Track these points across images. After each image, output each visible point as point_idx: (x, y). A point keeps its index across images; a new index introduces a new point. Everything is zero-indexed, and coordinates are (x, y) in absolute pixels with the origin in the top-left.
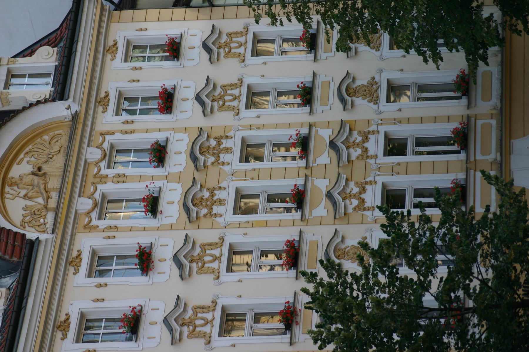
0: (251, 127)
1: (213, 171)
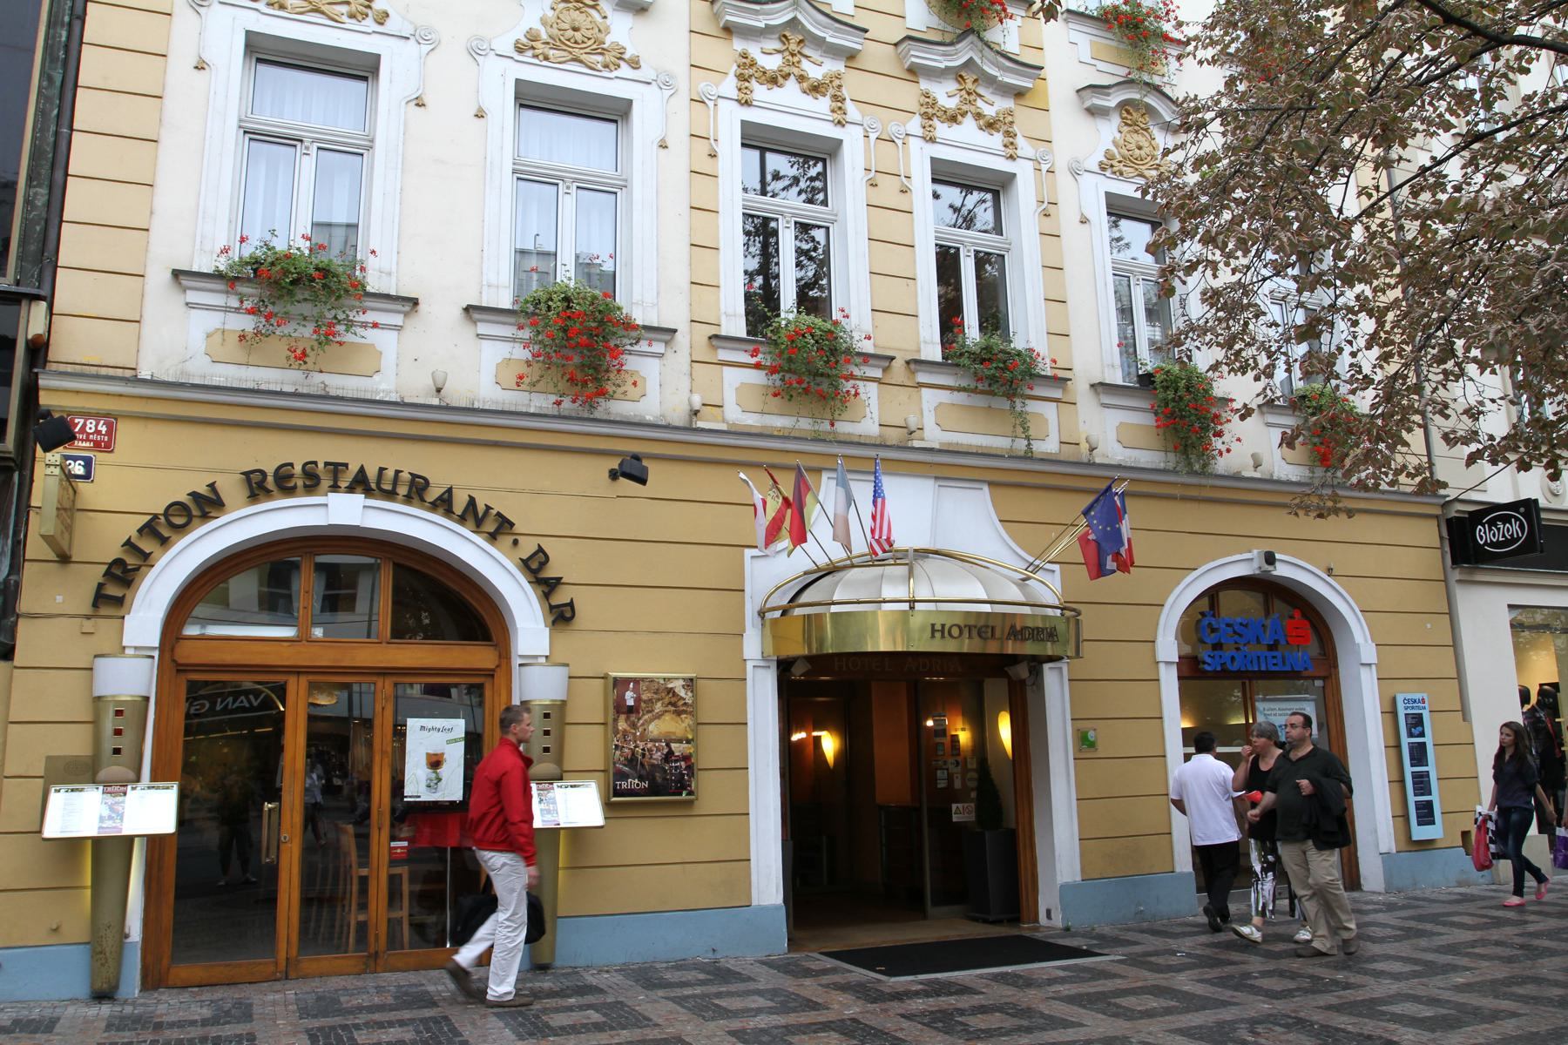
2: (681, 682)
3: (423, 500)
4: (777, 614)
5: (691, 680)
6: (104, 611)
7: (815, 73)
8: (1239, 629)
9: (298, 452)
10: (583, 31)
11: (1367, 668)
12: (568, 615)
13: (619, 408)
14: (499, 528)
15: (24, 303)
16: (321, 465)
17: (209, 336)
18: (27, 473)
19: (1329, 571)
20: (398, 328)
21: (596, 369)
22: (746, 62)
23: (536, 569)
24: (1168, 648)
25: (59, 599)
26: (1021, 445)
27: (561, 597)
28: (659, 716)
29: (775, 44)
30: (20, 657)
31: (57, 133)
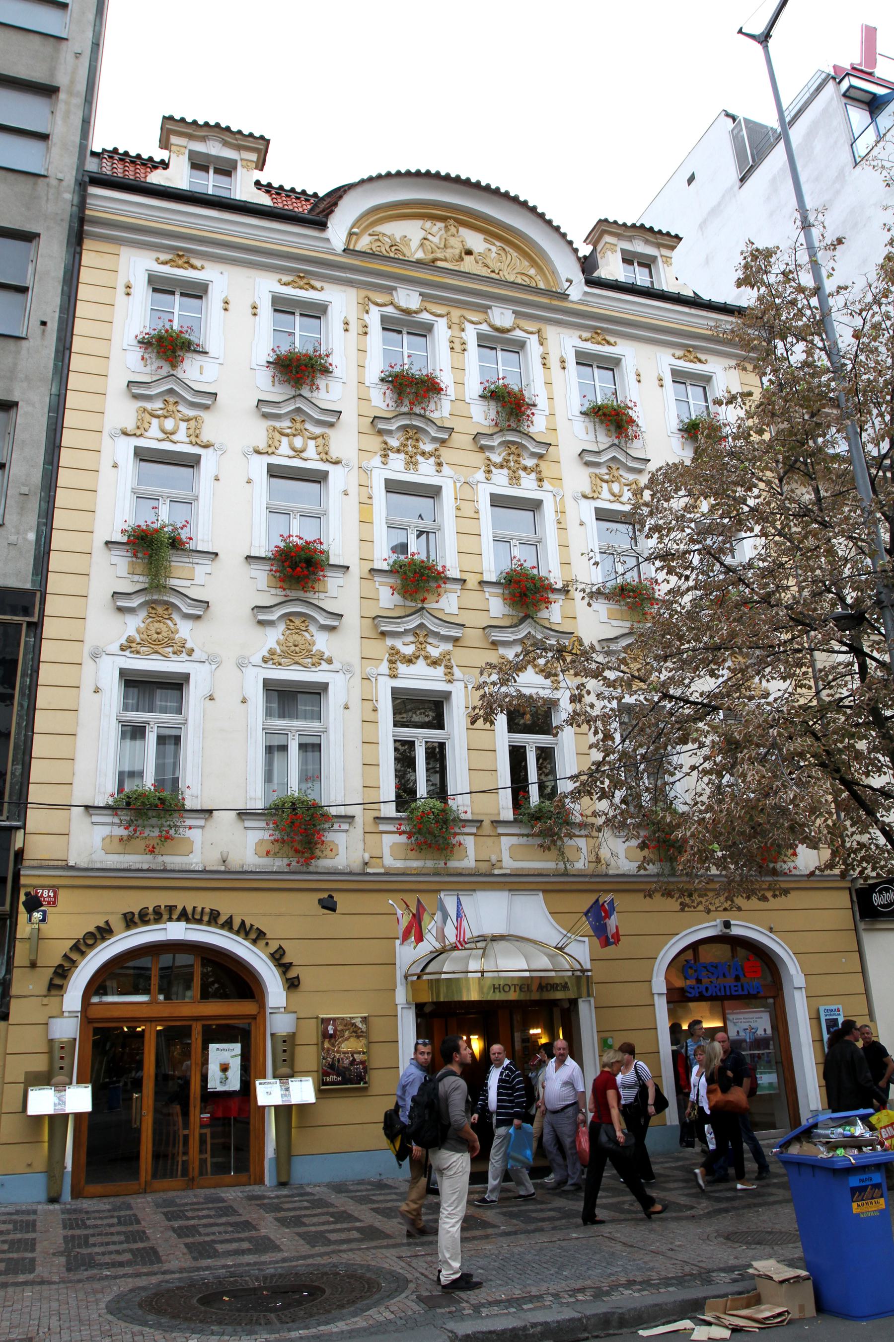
0: (561, 512)
1: (478, 459)
2: (360, 1019)
3: (216, 923)
4: (415, 978)
5: (365, 1017)
6: (53, 992)
7: (434, 652)
8: (713, 968)
9: (151, 900)
10: (300, 646)
11: (799, 991)
12: (296, 983)
13: (325, 863)
14: (257, 936)
15: (13, 831)
16: (163, 907)
17: (103, 839)
18: (14, 920)
19: (771, 930)
20: (202, 827)
21: (310, 843)
22: (394, 651)
23: (278, 958)
24: (659, 985)
25: (31, 987)
26: (561, 866)
27: (292, 974)
28: (347, 1039)
29: (411, 639)
30: (12, 1020)
31: (25, 735)
